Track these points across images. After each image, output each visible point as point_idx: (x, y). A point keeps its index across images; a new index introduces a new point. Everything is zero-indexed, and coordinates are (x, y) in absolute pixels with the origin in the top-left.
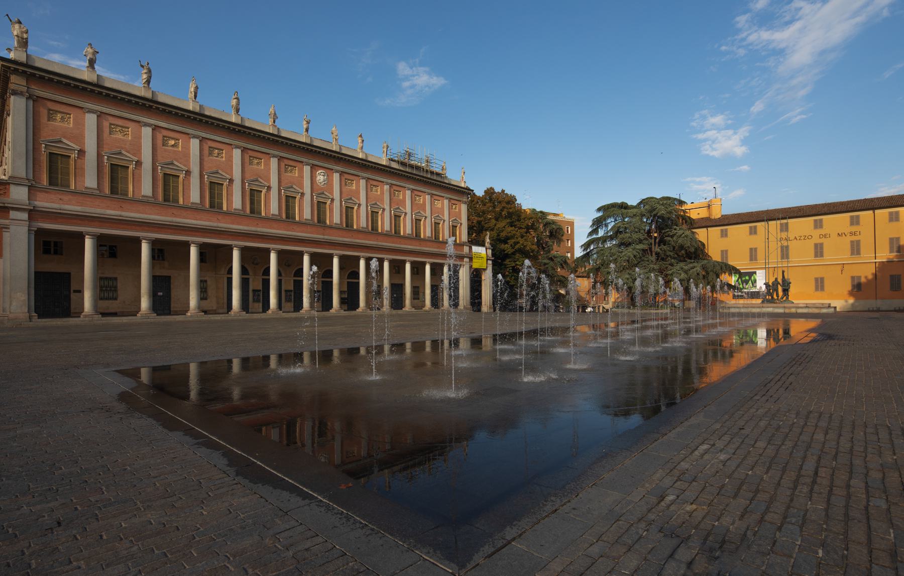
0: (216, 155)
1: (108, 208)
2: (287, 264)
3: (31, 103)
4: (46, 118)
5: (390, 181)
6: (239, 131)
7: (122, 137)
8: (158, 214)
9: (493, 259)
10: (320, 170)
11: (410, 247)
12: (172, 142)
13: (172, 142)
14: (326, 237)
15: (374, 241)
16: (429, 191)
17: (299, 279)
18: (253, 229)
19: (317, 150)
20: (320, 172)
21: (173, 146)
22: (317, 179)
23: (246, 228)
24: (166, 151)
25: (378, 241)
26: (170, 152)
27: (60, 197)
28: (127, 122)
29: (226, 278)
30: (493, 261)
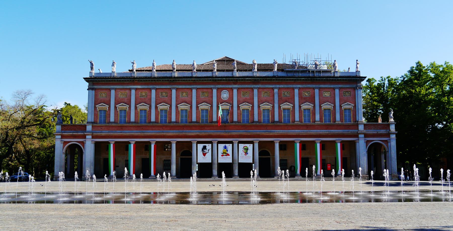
5: (278, 86)
9: (397, 133)
16: (317, 86)
17: (260, 157)
19: (219, 79)
20: (224, 91)
22: (221, 96)
25: (267, 130)
26: (142, 99)
29: (180, 158)
30: (396, 134)
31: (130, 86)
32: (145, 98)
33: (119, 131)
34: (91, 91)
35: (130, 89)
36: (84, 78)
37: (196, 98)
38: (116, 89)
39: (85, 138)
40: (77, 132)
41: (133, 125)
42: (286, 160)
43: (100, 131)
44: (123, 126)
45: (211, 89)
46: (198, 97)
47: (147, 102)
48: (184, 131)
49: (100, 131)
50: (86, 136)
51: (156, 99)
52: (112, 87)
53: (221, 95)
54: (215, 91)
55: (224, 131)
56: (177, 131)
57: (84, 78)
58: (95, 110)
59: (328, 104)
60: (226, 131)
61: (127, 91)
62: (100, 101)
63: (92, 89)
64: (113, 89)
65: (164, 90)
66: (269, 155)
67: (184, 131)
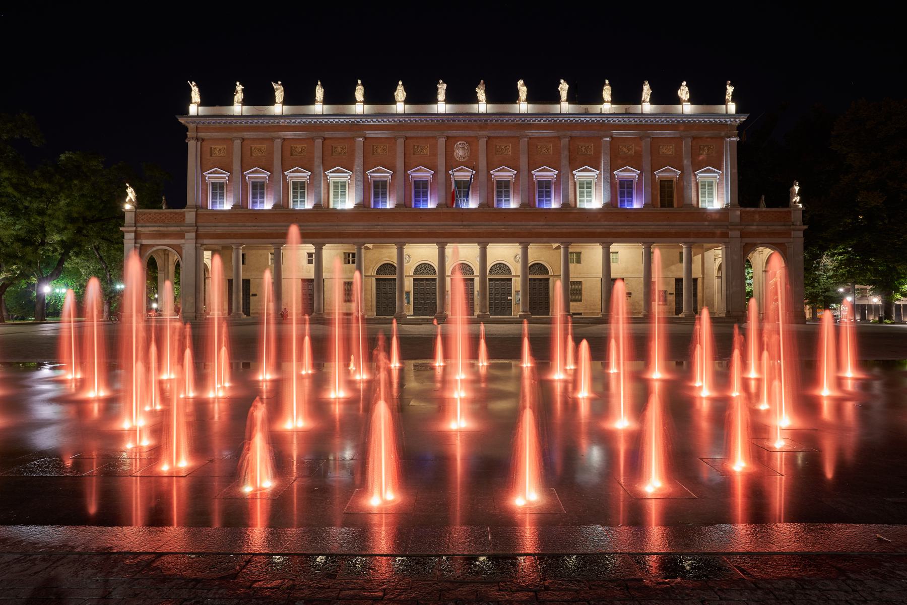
0: (340, 151)
4: (209, 155)
10: (458, 141)
20: (460, 142)
21: (301, 152)
22: (455, 153)
31: (272, 134)
33: (250, 224)
35: (272, 139)
40: (167, 227)
41: (278, 212)
42: (581, 282)
43: (213, 224)
44: (257, 214)
45: (434, 138)
48: (380, 224)
49: (213, 224)
50: (186, 234)
52: (235, 134)
53: (454, 151)
54: (442, 141)
55: (461, 223)
56: (366, 224)
59: (668, 170)
60: (465, 223)
66: (547, 273)
67: (380, 224)
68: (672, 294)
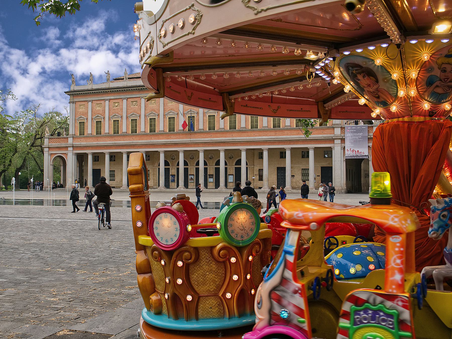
1: (94, 141)
2: (192, 158)
3: (74, 104)
6: (141, 89)
7: (100, 109)
8: (110, 141)
11: (264, 137)
12: (116, 104)
13: (116, 104)
14: (191, 139)
15: (230, 137)
18: (149, 141)
23: (145, 141)
24: (114, 109)
27: (80, 139)
28: (101, 101)
32: (117, 108)
34: (72, 104)
36: (65, 92)
37: (164, 106)
38: (92, 101)
39: (67, 150)
46: (165, 105)
47: (119, 112)
51: (127, 109)
57: (65, 92)
58: (75, 122)
61: (102, 102)
62: (80, 113)
63: (73, 102)
64: (90, 101)
65: (135, 99)
68: (319, 176)
